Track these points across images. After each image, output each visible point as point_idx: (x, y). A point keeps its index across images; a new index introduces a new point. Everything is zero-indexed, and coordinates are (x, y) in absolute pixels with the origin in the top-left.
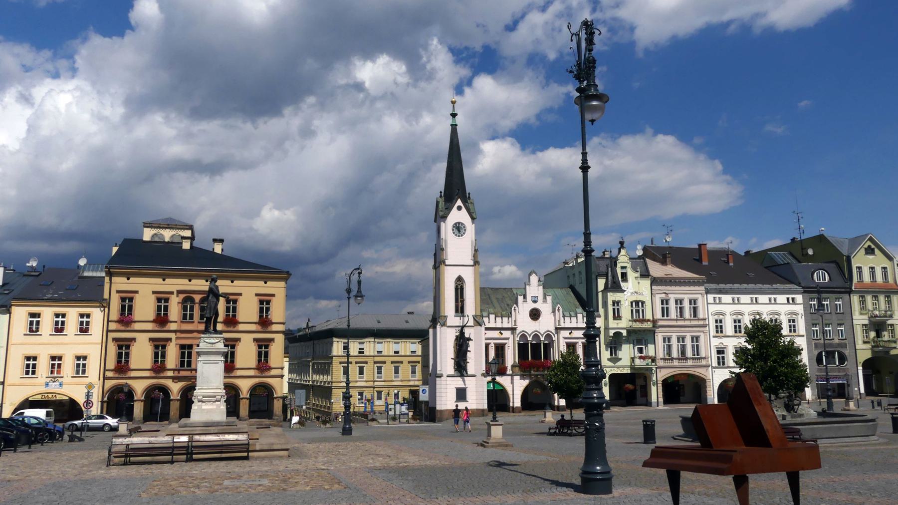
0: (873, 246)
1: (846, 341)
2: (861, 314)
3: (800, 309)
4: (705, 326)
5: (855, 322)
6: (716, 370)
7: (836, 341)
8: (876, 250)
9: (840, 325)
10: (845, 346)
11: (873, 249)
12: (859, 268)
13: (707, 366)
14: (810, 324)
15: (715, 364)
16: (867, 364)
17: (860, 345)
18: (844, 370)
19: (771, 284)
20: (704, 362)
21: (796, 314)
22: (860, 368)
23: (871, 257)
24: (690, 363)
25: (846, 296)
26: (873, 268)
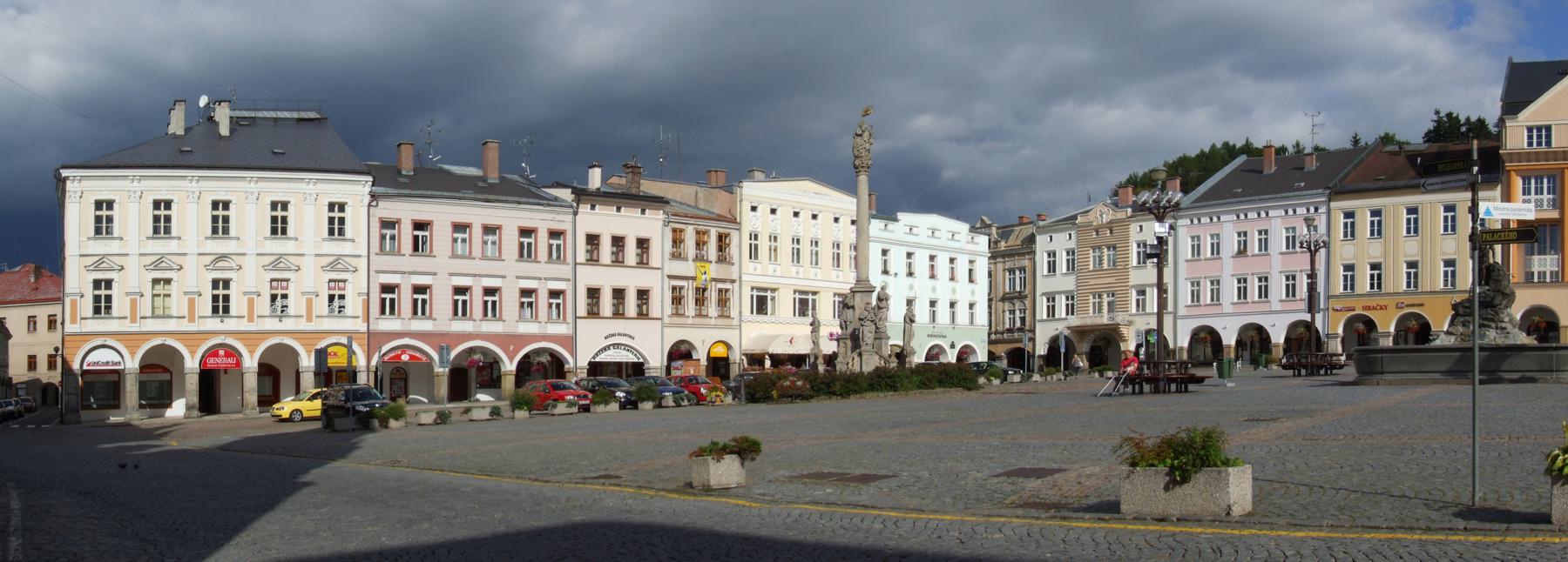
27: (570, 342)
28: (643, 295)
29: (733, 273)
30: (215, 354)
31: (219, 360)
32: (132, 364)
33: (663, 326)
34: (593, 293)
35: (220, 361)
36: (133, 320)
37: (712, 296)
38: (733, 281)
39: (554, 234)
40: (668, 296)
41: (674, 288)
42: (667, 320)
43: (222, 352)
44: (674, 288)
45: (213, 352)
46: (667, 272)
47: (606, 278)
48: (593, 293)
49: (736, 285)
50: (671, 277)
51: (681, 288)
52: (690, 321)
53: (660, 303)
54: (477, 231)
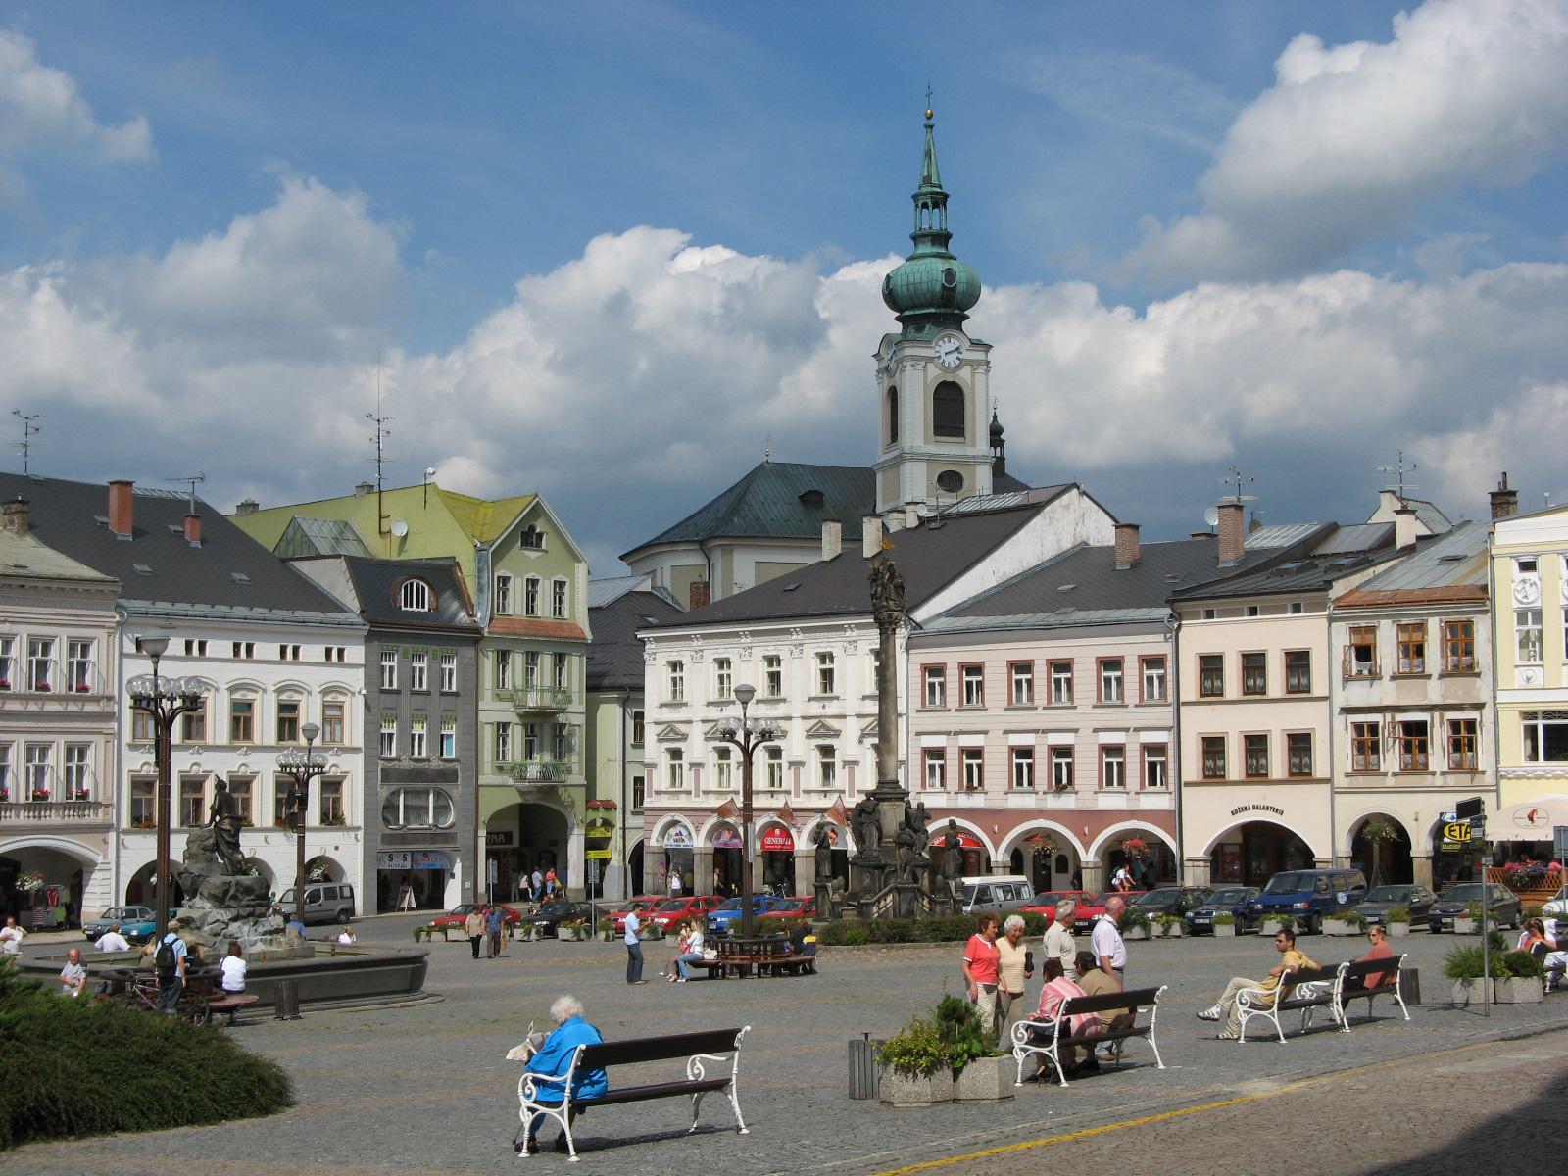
2: (498, 697)
4: (108, 717)
5: (483, 717)
6: (128, 839)
7: (436, 764)
11: (540, 536)
13: (106, 828)
15: (125, 822)
17: (488, 776)
19: (292, 608)
20: (92, 818)
22: (482, 833)
23: (533, 554)
24: (53, 818)
25: (468, 652)
26: (533, 583)
27: (1174, 819)
28: (1300, 743)
29: (1481, 689)
30: (772, 834)
31: (775, 841)
33: (1334, 792)
34: (1213, 747)
36: (697, 796)
37: (1439, 736)
38: (1479, 706)
39: (1153, 662)
40: (1345, 741)
41: (1359, 728)
42: (1340, 781)
43: (777, 831)
44: (1359, 727)
46: (1340, 701)
47: (1233, 721)
48: (1213, 747)
49: (1488, 712)
50: (1347, 710)
51: (1374, 728)
52: (1390, 781)
53: (1334, 752)
54: (1040, 673)
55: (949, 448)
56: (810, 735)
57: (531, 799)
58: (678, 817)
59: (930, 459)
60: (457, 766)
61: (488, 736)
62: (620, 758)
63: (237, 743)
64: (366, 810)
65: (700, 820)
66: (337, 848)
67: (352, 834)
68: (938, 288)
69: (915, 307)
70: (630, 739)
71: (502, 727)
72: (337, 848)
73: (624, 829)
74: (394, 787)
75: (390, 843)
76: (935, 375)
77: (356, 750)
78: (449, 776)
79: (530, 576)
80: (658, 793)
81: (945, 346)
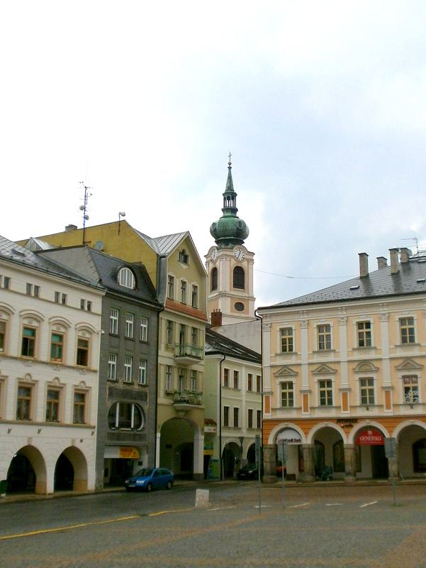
0: (187, 253)
1: (147, 390)
3: (96, 323)
7: (136, 387)
8: (190, 259)
9: (143, 361)
10: (143, 396)
11: (186, 257)
12: (171, 278)
14: (106, 354)
16: (166, 429)
17: (162, 399)
18: (141, 437)
21: (90, 331)
22: (159, 435)
23: (184, 266)
30: (366, 434)
31: (368, 438)
32: (307, 441)
35: (372, 438)
43: (370, 432)
45: (363, 432)
55: (238, 293)
56: (398, 369)
57: (181, 414)
58: (291, 425)
59: (232, 297)
60: (147, 390)
61: (162, 371)
62: (218, 395)
63: (25, 357)
64: (100, 415)
65: (307, 426)
66: (81, 441)
67: (91, 431)
68: (235, 228)
69: (224, 236)
70: (223, 385)
71: (169, 367)
72: (81, 441)
73: (220, 437)
74: (115, 401)
75: (112, 439)
76: (234, 264)
77: (95, 371)
78: (143, 396)
79: (181, 279)
80: (274, 410)
81: (236, 252)
